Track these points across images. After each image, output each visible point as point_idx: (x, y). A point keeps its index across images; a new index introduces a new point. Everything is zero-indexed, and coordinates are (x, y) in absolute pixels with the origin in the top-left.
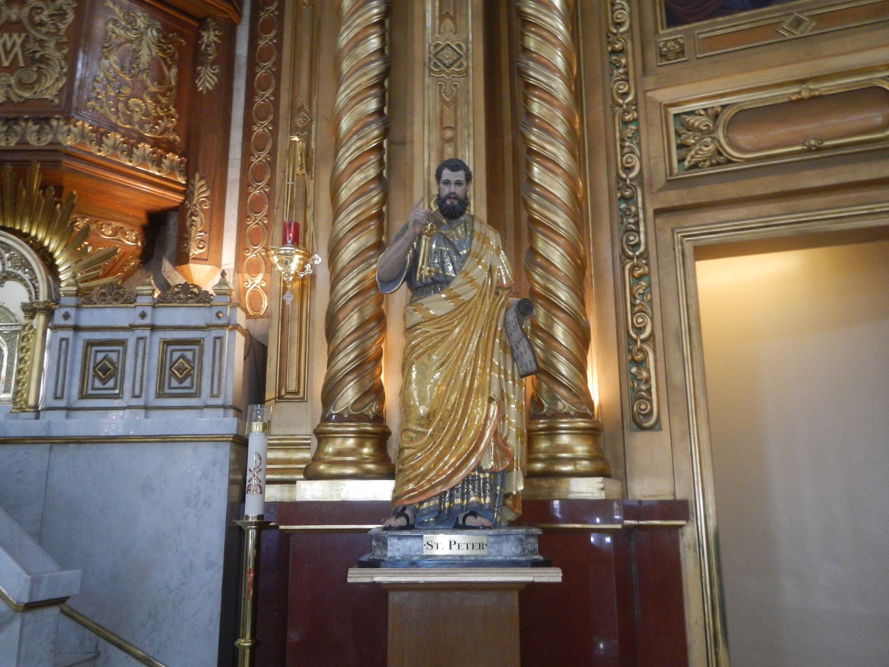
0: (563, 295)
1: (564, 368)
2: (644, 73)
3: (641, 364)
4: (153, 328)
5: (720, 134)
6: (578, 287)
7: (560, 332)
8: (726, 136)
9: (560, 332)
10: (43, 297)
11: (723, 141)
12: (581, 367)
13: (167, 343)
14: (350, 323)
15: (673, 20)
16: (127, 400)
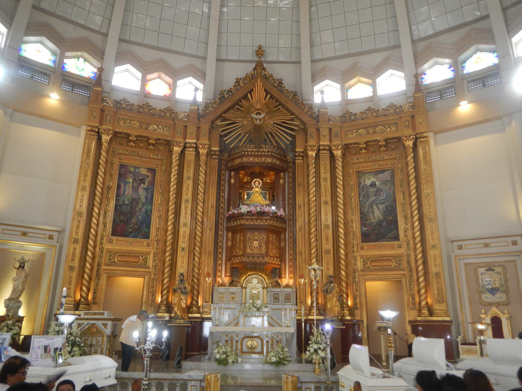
0: (344, 290)
1: (345, 301)
2: (358, 251)
3: (356, 299)
4: (283, 292)
5: (369, 263)
6: (347, 289)
7: (344, 295)
8: (370, 263)
9: (344, 295)
10: (266, 286)
11: (369, 265)
12: (347, 301)
13: (285, 294)
14: (314, 294)
15: (363, 242)
16: (280, 303)
